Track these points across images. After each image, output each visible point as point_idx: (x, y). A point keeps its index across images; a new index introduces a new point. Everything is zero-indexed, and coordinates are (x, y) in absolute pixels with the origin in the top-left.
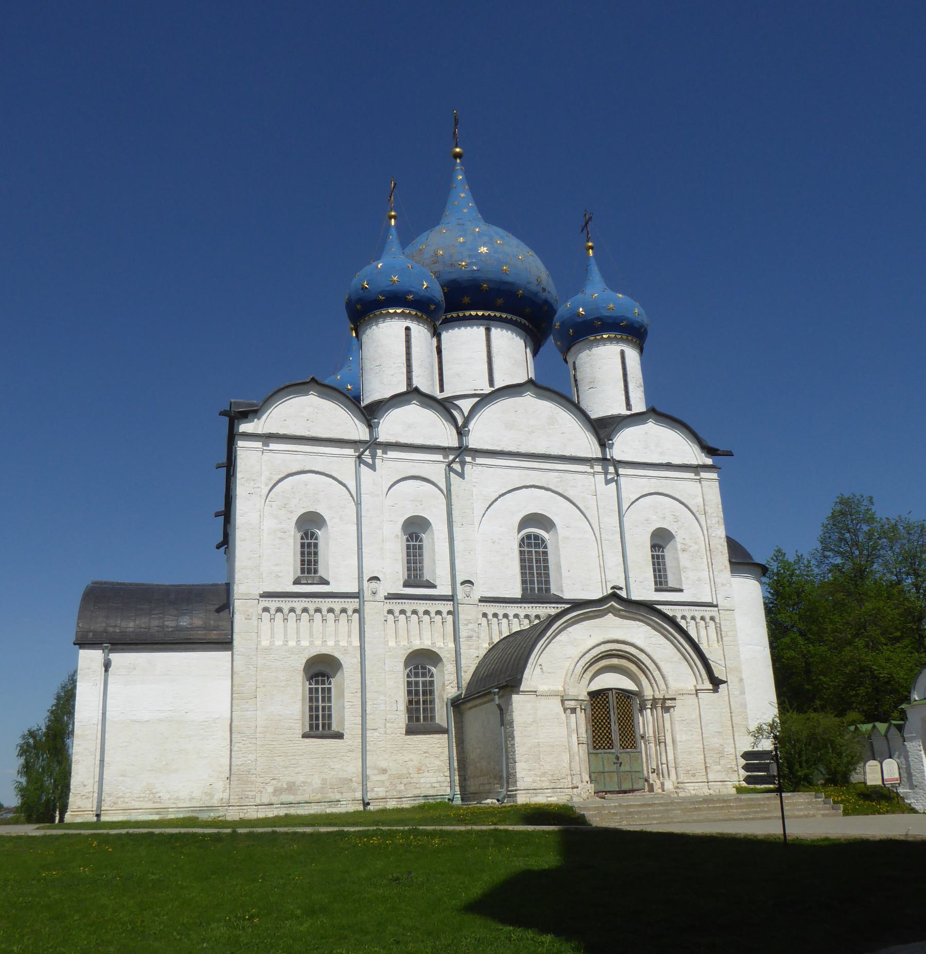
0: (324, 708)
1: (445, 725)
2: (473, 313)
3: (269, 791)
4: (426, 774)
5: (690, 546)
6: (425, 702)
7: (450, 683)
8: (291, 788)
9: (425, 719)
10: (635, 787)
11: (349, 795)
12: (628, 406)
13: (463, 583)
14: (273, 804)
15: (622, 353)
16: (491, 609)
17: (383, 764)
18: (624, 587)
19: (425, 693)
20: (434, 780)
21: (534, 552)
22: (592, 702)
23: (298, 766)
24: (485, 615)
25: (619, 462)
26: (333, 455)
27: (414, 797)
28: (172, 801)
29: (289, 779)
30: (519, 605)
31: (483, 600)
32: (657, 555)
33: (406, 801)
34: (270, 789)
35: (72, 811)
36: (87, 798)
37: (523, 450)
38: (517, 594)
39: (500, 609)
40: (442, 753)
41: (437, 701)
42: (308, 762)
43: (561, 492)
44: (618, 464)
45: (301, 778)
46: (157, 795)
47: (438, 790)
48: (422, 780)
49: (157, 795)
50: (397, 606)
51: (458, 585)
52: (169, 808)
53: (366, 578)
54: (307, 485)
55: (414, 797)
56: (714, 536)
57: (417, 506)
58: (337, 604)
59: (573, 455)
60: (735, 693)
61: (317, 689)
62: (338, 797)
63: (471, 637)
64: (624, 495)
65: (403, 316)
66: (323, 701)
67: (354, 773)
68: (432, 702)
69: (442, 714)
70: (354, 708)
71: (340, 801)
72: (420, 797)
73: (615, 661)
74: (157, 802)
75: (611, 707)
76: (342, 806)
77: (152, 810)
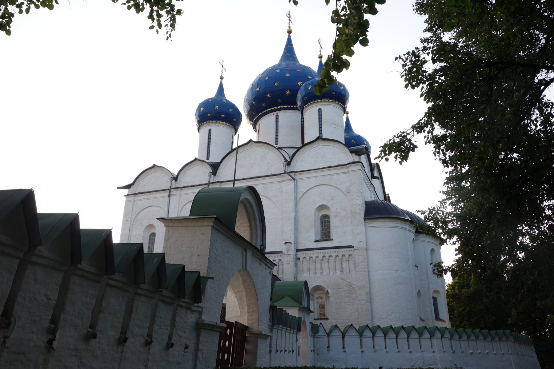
2: (268, 110)
18: (293, 243)
56: (355, 204)
59: (272, 174)
60: (362, 302)
64: (299, 190)
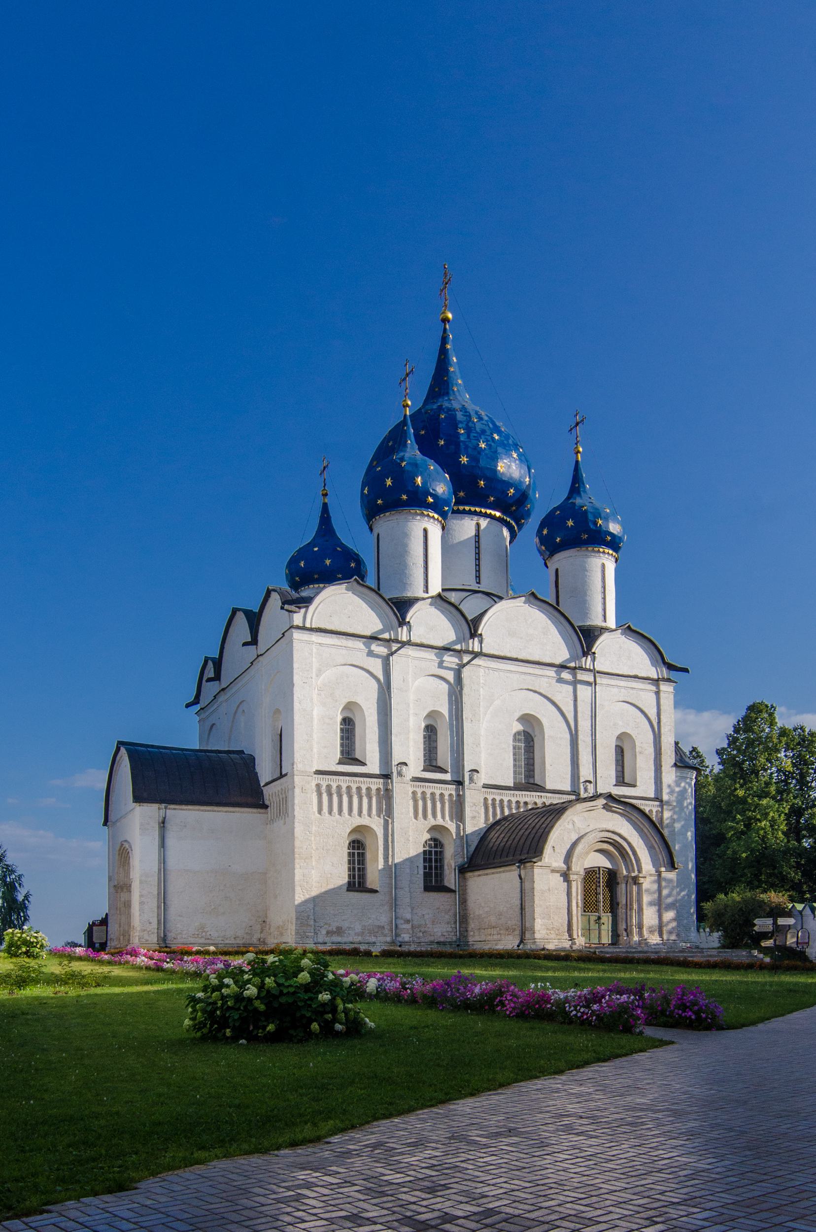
0: (359, 869)
1: (453, 887)
6: (436, 868)
8: (339, 931)
9: (436, 881)
11: (381, 939)
12: (605, 620)
14: (326, 943)
16: (492, 795)
17: (408, 916)
19: (436, 861)
24: (486, 799)
25: (598, 672)
29: (337, 924)
30: (512, 792)
31: (486, 786)
34: (324, 932)
36: (153, 933)
38: (511, 784)
39: (498, 796)
40: (449, 910)
41: (446, 867)
44: (595, 672)
45: (345, 925)
46: (208, 934)
49: (208, 934)
61: (354, 853)
62: (373, 939)
63: (475, 817)
66: (359, 864)
68: (442, 867)
69: (450, 879)
74: (208, 939)
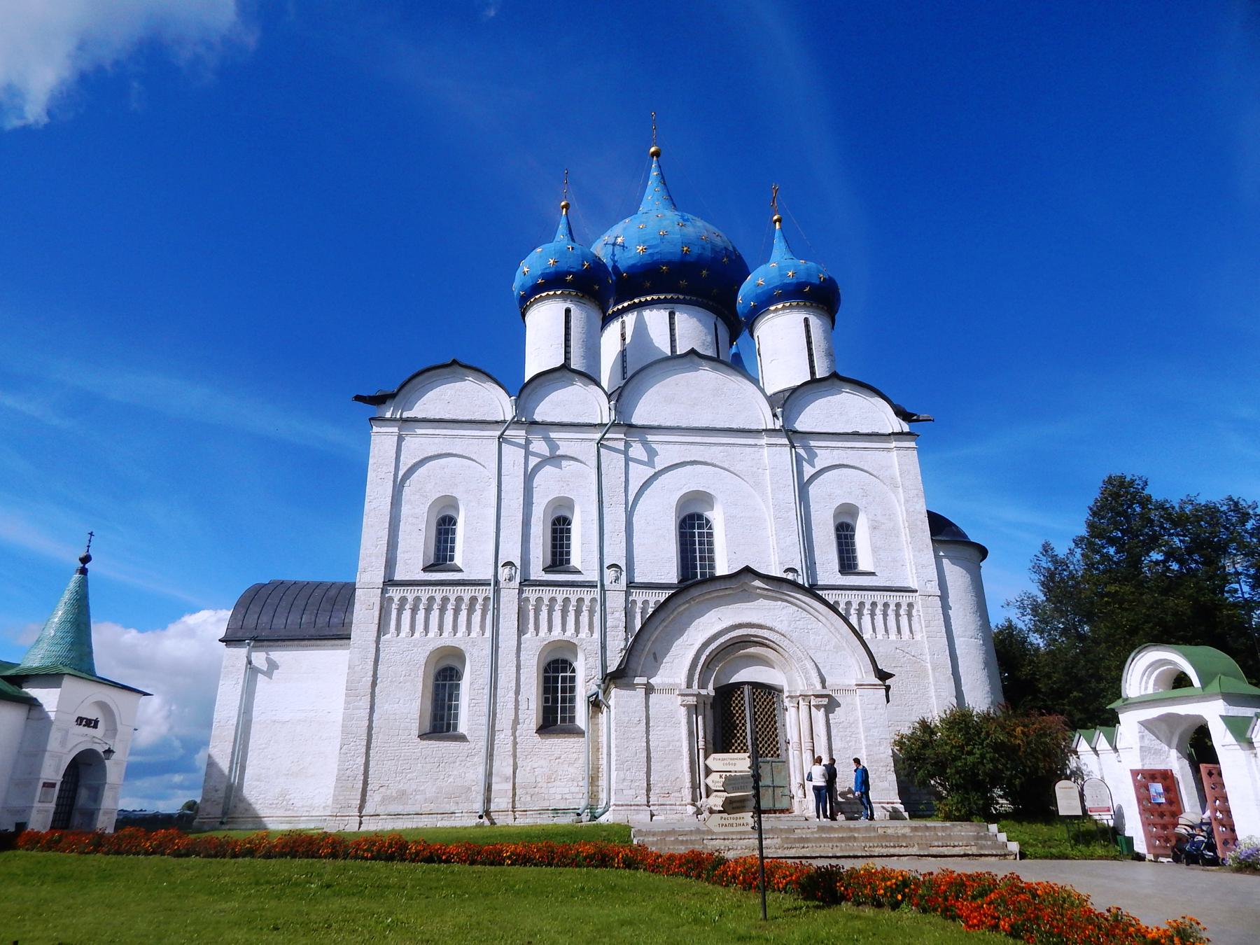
3: (376, 800)
4: (558, 783)
5: (884, 524)
7: (590, 679)
8: (402, 794)
9: (563, 720)
10: (778, 806)
11: (465, 807)
13: (609, 567)
15: (806, 320)
20: (566, 790)
21: (696, 533)
22: (723, 699)
23: (410, 772)
26: (474, 437)
27: (542, 810)
28: (305, 809)
32: (844, 535)
33: (530, 815)
35: (200, 818)
36: (217, 804)
37: (684, 424)
42: (422, 767)
43: (726, 467)
46: (291, 802)
47: (570, 803)
48: (552, 791)
50: (531, 594)
51: (605, 569)
52: (301, 817)
53: (500, 565)
54: (444, 468)
55: (542, 810)
56: (913, 511)
57: (563, 487)
58: (467, 593)
65: (564, 297)
67: (474, 781)
70: (479, 706)
71: (455, 813)
72: (548, 810)
73: (752, 650)
75: (747, 705)
76: (456, 819)
77: (283, 819)
